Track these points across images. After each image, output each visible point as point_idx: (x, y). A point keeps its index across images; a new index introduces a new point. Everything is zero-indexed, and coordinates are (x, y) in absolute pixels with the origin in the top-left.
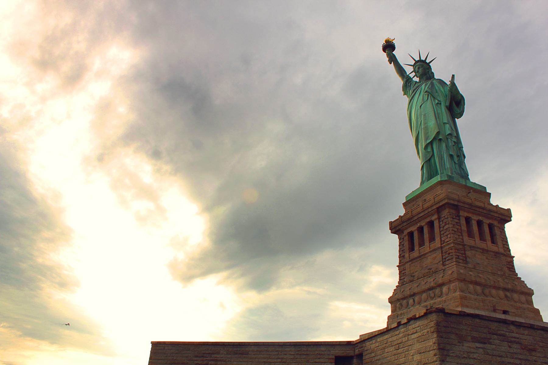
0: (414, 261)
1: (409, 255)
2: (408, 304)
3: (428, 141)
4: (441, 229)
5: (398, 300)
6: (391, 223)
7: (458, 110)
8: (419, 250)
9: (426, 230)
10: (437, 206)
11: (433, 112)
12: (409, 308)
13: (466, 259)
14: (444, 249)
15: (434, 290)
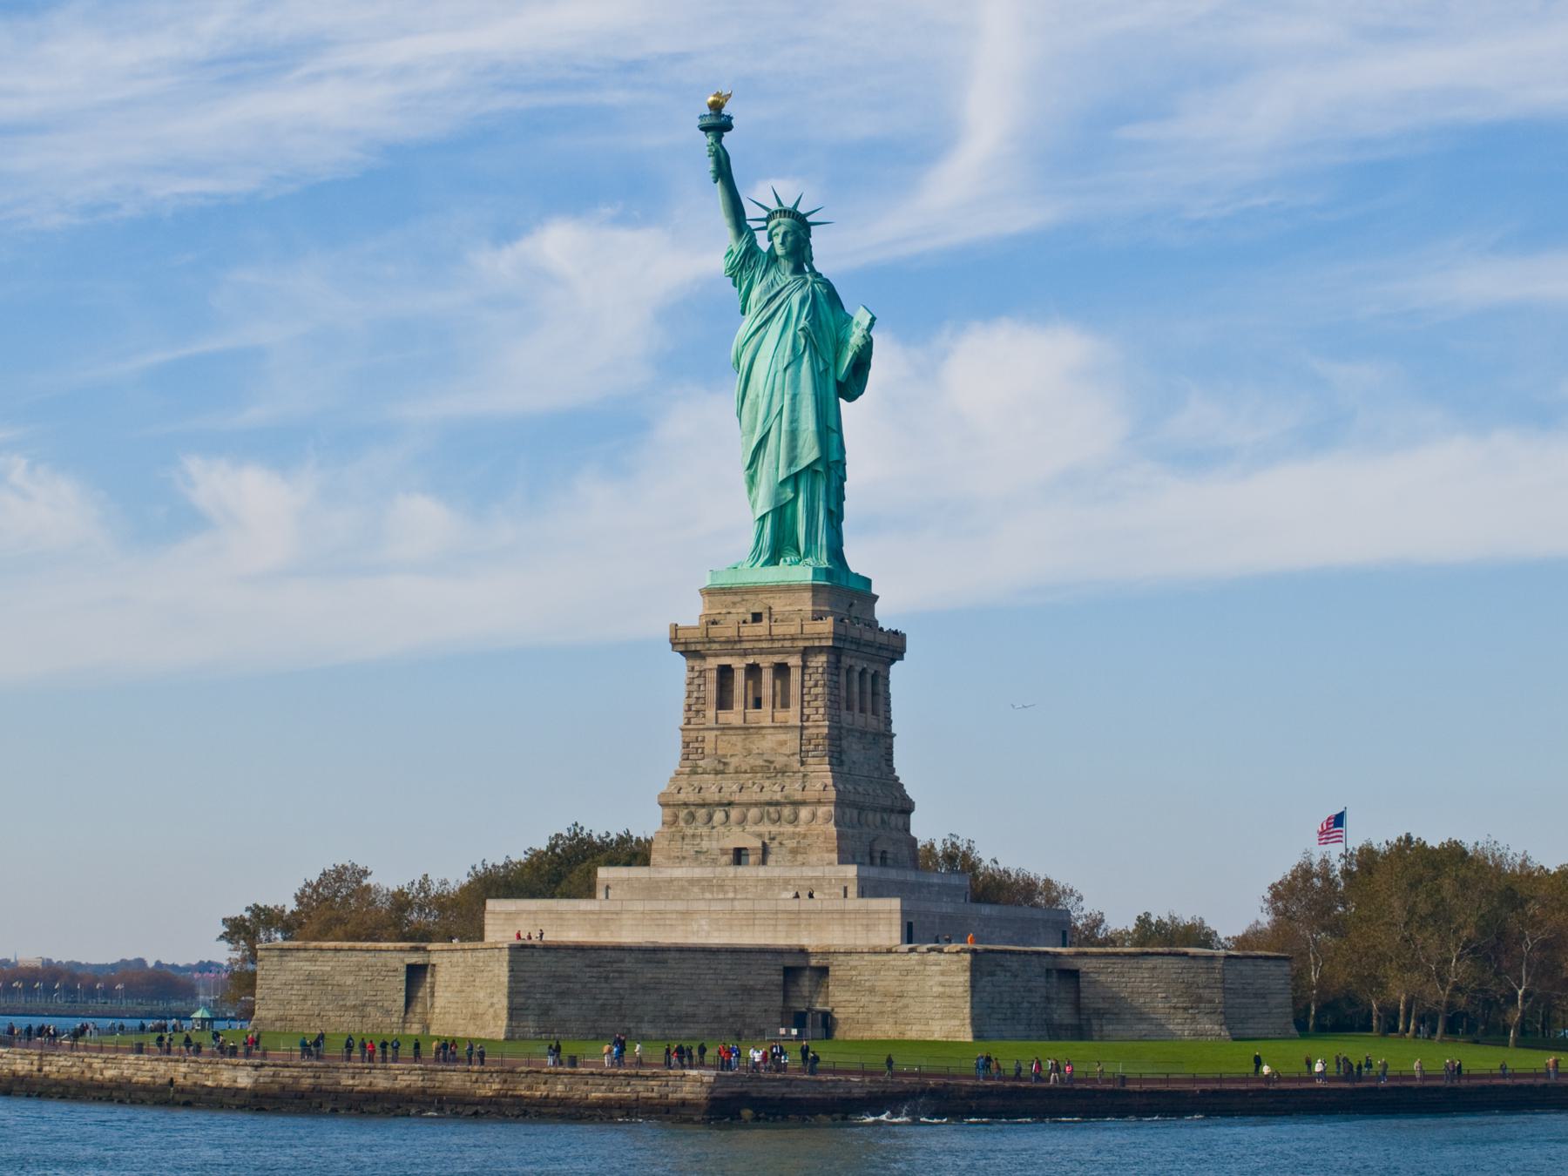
0: (731, 732)
1: (717, 714)
2: (710, 818)
3: (794, 470)
4: (805, 690)
5: (686, 805)
6: (675, 628)
7: (856, 388)
8: (745, 714)
9: (767, 677)
10: (807, 644)
11: (813, 398)
12: (713, 828)
13: (841, 755)
14: (805, 732)
15: (779, 808)
